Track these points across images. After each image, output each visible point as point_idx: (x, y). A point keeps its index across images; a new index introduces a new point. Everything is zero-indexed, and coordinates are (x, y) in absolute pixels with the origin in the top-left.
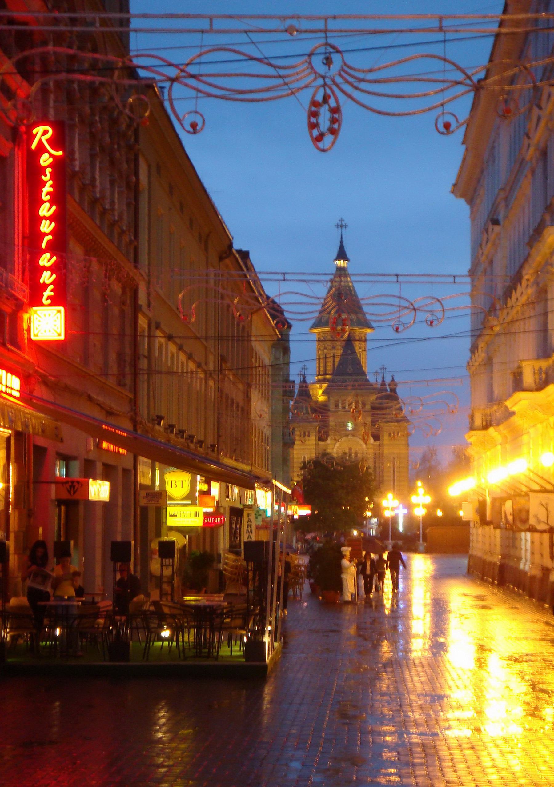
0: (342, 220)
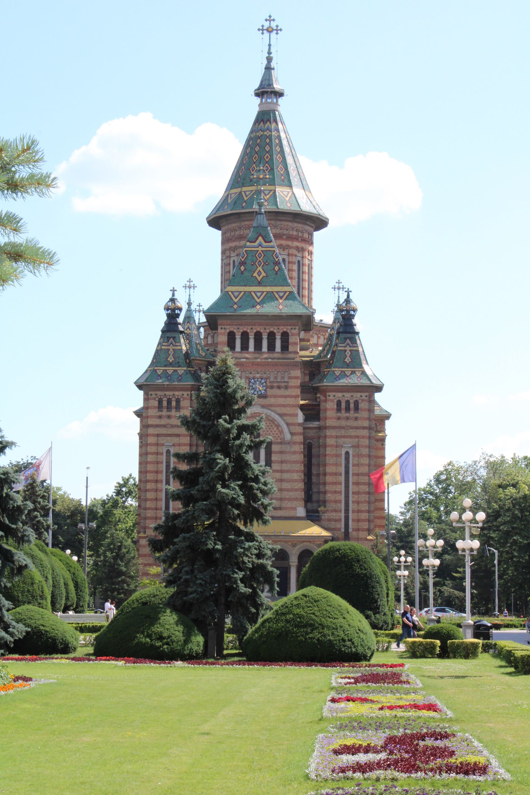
0: (270, 19)
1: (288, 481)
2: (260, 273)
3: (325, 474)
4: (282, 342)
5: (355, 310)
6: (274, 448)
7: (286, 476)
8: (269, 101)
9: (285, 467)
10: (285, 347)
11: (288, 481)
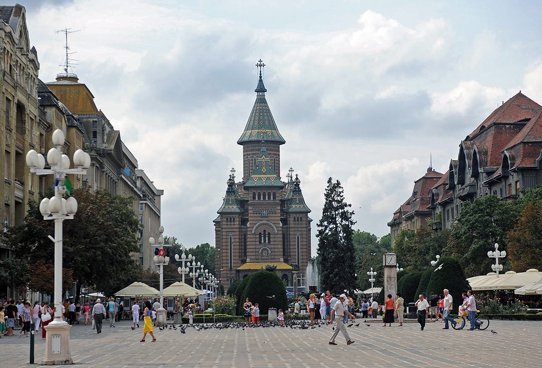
0: (260, 61)
1: (276, 248)
2: (264, 170)
3: (290, 245)
4: (273, 196)
5: (300, 182)
6: (271, 236)
7: (276, 246)
8: (261, 94)
9: (276, 243)
10: (274, 198)
11: (276, 248)
